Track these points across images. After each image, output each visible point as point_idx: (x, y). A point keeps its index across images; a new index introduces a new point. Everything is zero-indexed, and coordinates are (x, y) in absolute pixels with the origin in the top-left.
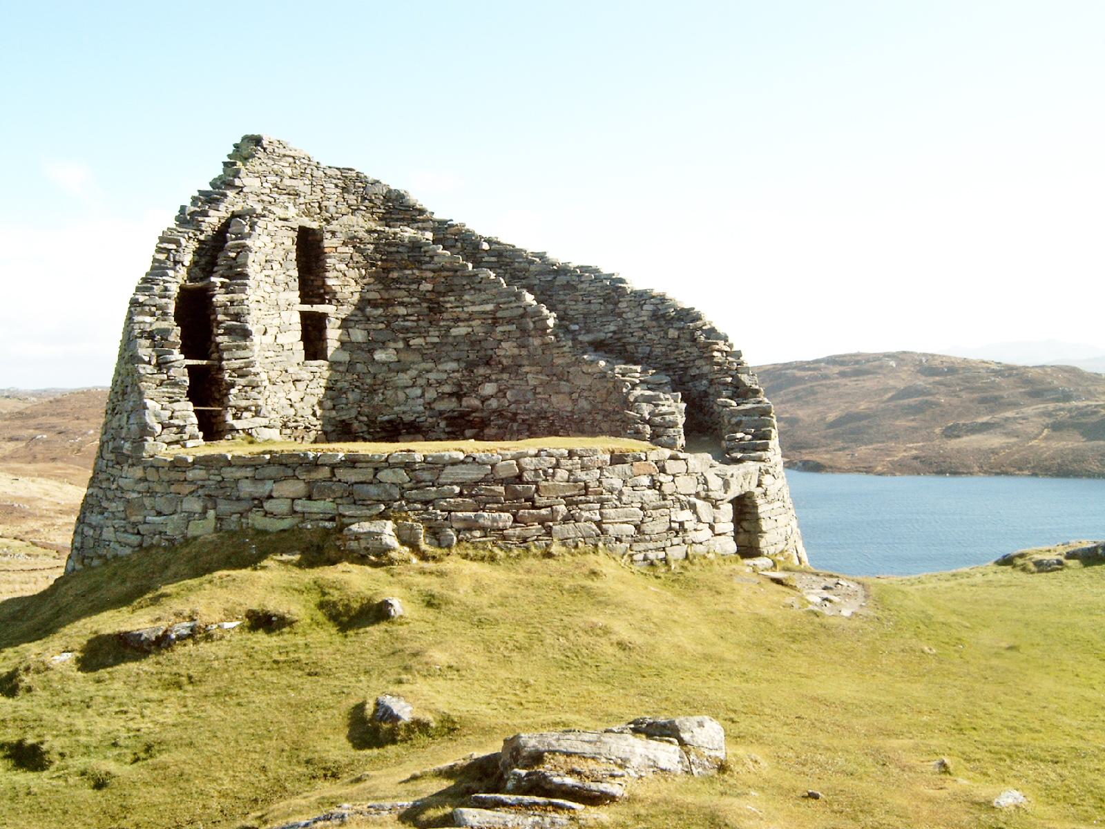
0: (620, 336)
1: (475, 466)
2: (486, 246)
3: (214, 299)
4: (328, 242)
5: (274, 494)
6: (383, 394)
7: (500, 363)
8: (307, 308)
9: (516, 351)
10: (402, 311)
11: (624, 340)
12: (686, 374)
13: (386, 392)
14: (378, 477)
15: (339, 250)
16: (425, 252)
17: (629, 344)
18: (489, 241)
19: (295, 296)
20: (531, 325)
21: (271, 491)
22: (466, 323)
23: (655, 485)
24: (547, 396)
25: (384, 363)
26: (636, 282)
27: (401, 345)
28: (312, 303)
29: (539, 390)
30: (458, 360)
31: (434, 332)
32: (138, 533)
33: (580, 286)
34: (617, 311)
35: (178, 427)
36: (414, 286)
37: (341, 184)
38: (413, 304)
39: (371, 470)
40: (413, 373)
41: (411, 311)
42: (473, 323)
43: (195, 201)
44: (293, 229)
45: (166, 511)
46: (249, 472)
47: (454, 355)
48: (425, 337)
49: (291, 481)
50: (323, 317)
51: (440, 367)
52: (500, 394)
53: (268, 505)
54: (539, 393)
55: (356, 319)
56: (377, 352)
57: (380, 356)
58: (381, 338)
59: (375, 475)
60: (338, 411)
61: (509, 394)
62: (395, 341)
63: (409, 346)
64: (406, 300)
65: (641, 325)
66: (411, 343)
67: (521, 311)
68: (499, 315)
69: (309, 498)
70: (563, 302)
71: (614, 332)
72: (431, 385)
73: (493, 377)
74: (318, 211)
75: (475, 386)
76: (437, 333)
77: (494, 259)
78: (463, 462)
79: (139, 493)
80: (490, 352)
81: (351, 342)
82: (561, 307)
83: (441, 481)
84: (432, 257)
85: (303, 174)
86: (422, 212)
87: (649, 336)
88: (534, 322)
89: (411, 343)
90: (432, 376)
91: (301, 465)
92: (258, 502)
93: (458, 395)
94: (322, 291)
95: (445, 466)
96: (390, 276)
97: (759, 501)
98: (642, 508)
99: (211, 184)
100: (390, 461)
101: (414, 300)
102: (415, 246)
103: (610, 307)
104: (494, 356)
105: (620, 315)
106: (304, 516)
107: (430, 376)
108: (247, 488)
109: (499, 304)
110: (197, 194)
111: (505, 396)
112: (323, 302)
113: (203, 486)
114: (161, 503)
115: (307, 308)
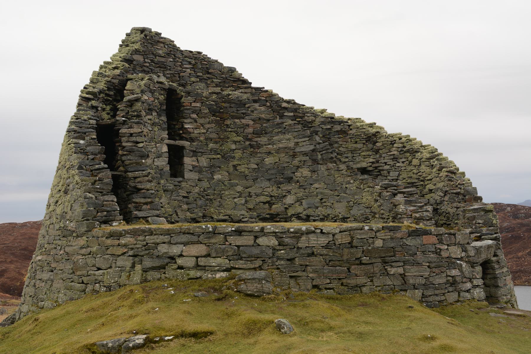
0: (377, 165)
1: (321, 235)
2: (284, 105)
3: (120, 131)
4: (186, 100)
5: (184, 254)
7: (298, 181)
8: (172, 142)
10: (233, 147)
11: (381, 168)
12: (425, 188)
14: (257, 241)
15: (194, 104)
16: (249, 107)
17: (383, 170)
18: (289, 102)
19: (165, 135)
20: (320, 157)
21: (182, 251)
23: (438, 252)
24: (329, 204)
25: (219, 180)
27: (231, 169)
28: (175, 140)
30: (269, 180)
32: (83, 283)
33: (351, 132)
35: (108, 211)
37: (193, 62)
39: (253, 237)
43: (101, 67)
44: (164, 89)
45: (103, 267)
46: (166, 238)
49: (196, 246)
50: (183, 148)
52: (298, 203)
53: (180, 261)
54: (325, 202)
59: (255, 241)
63: (237, 170)
65: (392, 157)
66: (237, 168)
67: (312, 147)
69: (208, 255)
70: (337, 142)
71: (373, 163)
72: (251, 196)
74: (178, 79)
75: (281, 197)
76: (256, 162)
77: (292, 114)
78: (314, 232)
79: (83, 255)
80: (292, 175)
82: (336, 145)
83: (300, 245)
84: (252, 111)
85: (169, 54)
86: (245, 82)
87: (398, 165)
89: (237, 168)
91: (203, 233)
92: (172, 258)
94: (181, 132)
95: (302, 234)
96: (225, 123)
97: (496, 266)
98: (429, 267)
99: (111, 58)
100: (265, 231)
102: (241, 104)
105: (377, 151)
106: (203, 268)
108: (163, 249)
110: (102, 64)
111: (301, 204)
112: (182, 138)
113: (132, 249)
114: (99, 262)
115: (172, 142)
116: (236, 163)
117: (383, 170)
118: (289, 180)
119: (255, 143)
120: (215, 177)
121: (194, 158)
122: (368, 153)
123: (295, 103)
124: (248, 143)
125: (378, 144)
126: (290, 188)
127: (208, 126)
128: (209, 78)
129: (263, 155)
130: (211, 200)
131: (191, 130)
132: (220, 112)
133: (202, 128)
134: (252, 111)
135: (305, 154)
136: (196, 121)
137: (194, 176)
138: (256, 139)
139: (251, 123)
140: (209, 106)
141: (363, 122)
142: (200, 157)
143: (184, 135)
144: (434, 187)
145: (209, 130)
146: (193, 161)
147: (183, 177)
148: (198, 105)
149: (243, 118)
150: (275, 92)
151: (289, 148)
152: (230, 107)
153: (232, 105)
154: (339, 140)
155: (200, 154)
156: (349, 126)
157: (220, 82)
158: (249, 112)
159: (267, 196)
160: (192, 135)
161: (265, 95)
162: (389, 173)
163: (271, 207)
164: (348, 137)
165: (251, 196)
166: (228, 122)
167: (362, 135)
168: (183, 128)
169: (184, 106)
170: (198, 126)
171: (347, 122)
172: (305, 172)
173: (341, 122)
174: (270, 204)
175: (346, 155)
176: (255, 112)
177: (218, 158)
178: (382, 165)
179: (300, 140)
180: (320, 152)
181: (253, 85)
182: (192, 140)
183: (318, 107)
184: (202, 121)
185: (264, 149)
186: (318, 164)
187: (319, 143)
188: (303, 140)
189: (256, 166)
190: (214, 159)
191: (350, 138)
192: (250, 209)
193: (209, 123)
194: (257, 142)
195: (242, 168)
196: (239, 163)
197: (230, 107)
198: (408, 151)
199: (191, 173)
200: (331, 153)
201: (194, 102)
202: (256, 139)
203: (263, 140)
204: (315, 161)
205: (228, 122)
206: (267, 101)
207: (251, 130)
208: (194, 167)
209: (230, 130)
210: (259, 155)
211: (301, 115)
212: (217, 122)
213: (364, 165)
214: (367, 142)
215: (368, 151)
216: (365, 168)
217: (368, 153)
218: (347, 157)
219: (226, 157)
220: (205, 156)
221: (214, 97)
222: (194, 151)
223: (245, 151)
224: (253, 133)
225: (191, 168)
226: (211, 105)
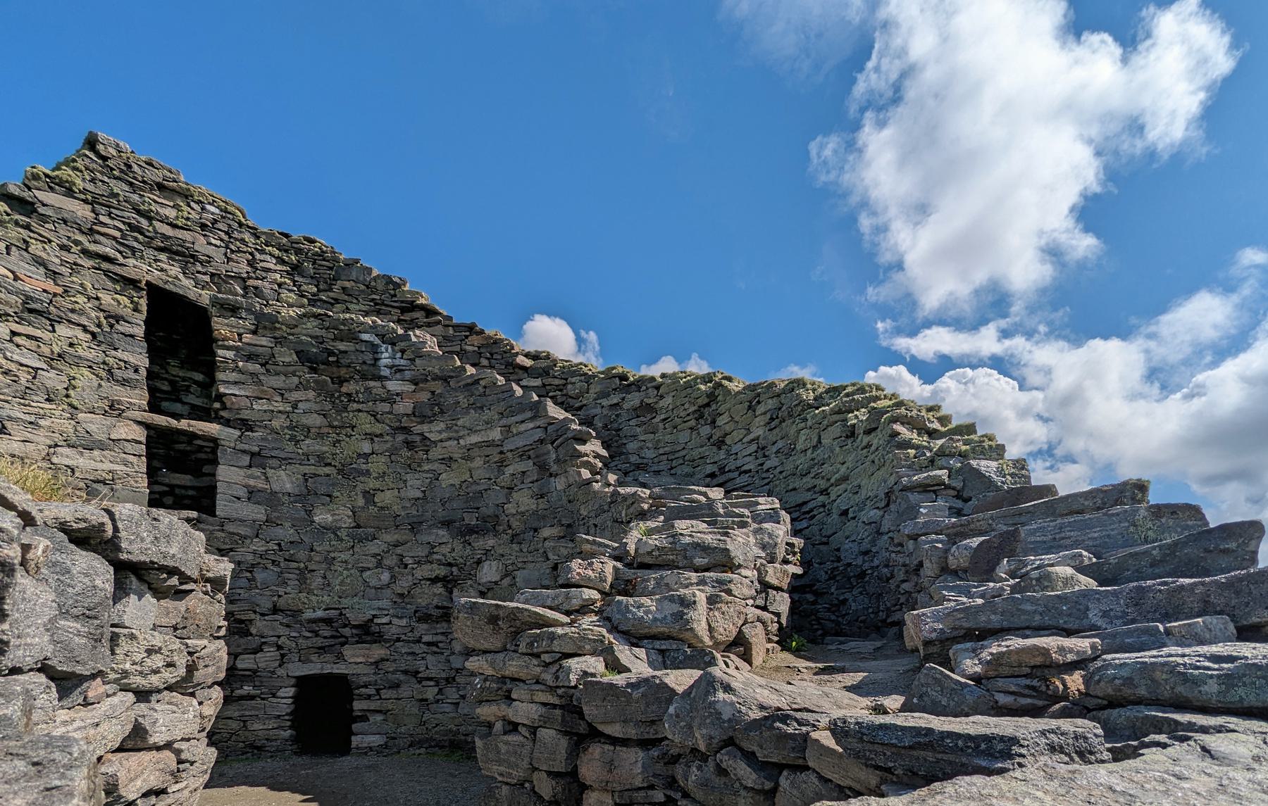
36: (385, 407)
38: (381, 435)
57: (322, 517)
72: (406, 566)
81: (273, 493)
96: (344, 389)
107: (399, 550)
116: (372, 484)
121: (256, 472)
124: (400, 437)
127: (295, 396)
129: (435, 466)
133: (279, 399)
136: (260, 383)
137: (257, 512)
138: (418, 429)
140: (300, 348)
145: (300, 405)
148: (264, 341)
154: (638, 430)
165: (406, 566)
170: (263, 391)
175: (655, 468)
184: (278, 382)
185: (436, 453)
192: (401, 595)
193: (297, 388)
194: (422, 434)
195: (385, 498)
202: (418, 429)
203: (434, 430)
205: (349, 388)
207: (405, 407)
208: (252, 493)
212: (320, 388)
221: (311, 325)
222: (253, 454)
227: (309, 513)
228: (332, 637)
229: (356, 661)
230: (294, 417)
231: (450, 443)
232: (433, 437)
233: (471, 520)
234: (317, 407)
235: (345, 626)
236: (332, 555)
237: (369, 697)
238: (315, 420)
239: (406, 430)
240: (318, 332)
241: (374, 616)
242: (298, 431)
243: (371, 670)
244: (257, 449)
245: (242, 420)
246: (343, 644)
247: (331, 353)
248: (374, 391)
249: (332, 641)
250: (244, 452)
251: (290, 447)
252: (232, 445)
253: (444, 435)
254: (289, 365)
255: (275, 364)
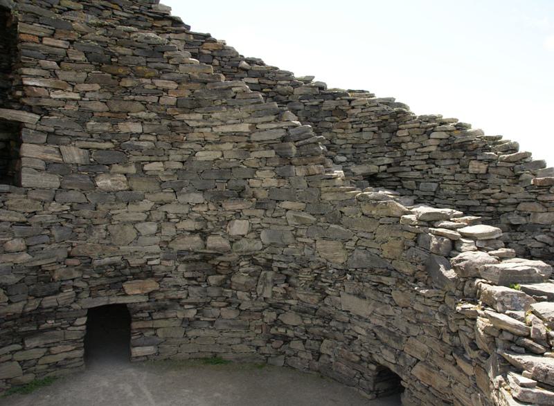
6: (107, 230)
9: (274, 183)
10: (137, 128)
11: (401, 175)
13: (110, 228)
16: (169, 58)
17: (406, 179)
18: (251, 61)
20: (294, 150)
22: (215, 147)
26: (419, 108)
27: (132, 170)
29: (300, 232)
30: (203, 191)
31: (175, 156)
33: (352, 111)
34: (394, 140)
36: (155, 99)
38: (150, 120)
40: (147, 205)
41: (146, 129)
42: (223, 147)
47: (198, 184)
48: (163, 162)
50: (18, 126)
51: (180, 199)
52: (252, 235)
54: (301, 236)
55: (73, 134)
56: (100, 178)
58: (105, 159)
60: (33, 253)
61: (263, 235)
62: (126, 164)
64: (143, 115)
65: (426, 157)
66: (146, 168)
67: (282, 133)
68: (255, 137)
71: (389, 165)
73: (246, 213)
75: (223, 223)
76: (179, 157)
80: (244, 183)
81: (64, 164)
84: (177, 65)
86: (177, 22)
88: (298, 147)
90: (171, 209)
93: (204, 234)
94: (19, 93)
96: (122, 84)
101: (153, 115)
102: (156, 51)
103: (386, 136)
104: (247, 187)
105: (398, 146)
107: (165, 208)
109: (256, 124)
111: (258, 238)
117: (406, 179)
118: (240, 194)
119: (179, 124)
120: (98, 183)
121: (51, 148)
122: (380, 149)
123: (262, 64)
124: (165, 122)
125: (399, 133)
126: (240, 206)
127: (85, 87)
128: (106, 8)
129: (193, 146)
130: (89, 227)
131: (44, 92)
132: (111, 63)
133: (70, 89)
134: (177, 65)
135: (269, 146)
136: (56, 76)
137: (53, 181)
139: (173, 85)
140: (87, 49)
141: (372, 96)
142: (63, 144)
143: (24, 100)
144: (523, 220)
145: (87, 95)
146: (47, 152)
147: (18, 185)
148: (61, 43)
149: (159, 78)
150: (229, 44)
151: (240, 134)
152: (134, 55)
153: (136, 52)
155: (66, 140)
156: (350, 101)
157: (128, 18)
158: (170, 66)
159: (197, 220)
160: (45, 102)
161: (211, 46)
162: (417, 184)
163: (205, 239)
164: (348, 120)
166: (128, 83)
167: (372, 118)
168: (21, 86)
169: (23, 41)
170: (59, 83)
171: (347, 95)
172: (266, 180)
173: (335, 95)
174: (204, 234)
176: (181, 66)
177: (108, 149)
178: (405, 169)
179: (260, 120)
180: (295, 142)
181: (192, 30)
182: (44, 111)
183: (299, 74)
184: (70, 76)
185: (194, 136)
186: (291, 164)
187: (295, 126)
188: (265, 119)
189: (179, 165)
190: (98, 149)
191: (351, 122)
192: (167, 242)
193: (86, 81)
194: (183, 121)
196: (147, 158)
197: (134, 55)
198: (462, 146)
199: (39, 176)
200: (316, 143)
201: (52, 36)
203: (193, 119)
204: (285, 158)
205: (128, 83)
206: (214, 57)
207: (171, 99)
208: (49, 165)
209: (132, 97)
210: (185, 146)
211: (270, 82)
213: (373, 169)
214: (379, 129)
215: (380, 145)
216: (376, 174)
217: (380, 149)
218: (344, 155)
219: (122, 150)
220: (77, 144)
222: (49, 133)
223: (160, 137)
224: (177, 105)
225: (41, 166)
226: (94, 47)
227: (93, 179)
228: (115, 276)
229: (134, 293)
230: (81, 103)
231: (206, 130)
232: (192, 124)
233: (222, 187)
234: (101, 97)
235: (125, 267)
236: (112, 212)
237: (143, 319)
238: (98, 107)
239: (171, 117)
240: (104, 39)
241: (148, 260)
242: (83, 116)
243: (144, 299)
244: (52, 130)
245: (41, 106)
246: (123, 281)
247: (113, 56)
248: (147, 87)
249: (115, 280)
250: (42, 132)
251: (77, 127)
252: (34, 127)
253: (201, 124)
254: (80, 62)
255: (69, 61)
